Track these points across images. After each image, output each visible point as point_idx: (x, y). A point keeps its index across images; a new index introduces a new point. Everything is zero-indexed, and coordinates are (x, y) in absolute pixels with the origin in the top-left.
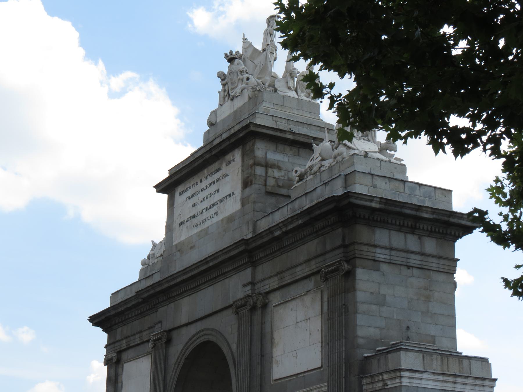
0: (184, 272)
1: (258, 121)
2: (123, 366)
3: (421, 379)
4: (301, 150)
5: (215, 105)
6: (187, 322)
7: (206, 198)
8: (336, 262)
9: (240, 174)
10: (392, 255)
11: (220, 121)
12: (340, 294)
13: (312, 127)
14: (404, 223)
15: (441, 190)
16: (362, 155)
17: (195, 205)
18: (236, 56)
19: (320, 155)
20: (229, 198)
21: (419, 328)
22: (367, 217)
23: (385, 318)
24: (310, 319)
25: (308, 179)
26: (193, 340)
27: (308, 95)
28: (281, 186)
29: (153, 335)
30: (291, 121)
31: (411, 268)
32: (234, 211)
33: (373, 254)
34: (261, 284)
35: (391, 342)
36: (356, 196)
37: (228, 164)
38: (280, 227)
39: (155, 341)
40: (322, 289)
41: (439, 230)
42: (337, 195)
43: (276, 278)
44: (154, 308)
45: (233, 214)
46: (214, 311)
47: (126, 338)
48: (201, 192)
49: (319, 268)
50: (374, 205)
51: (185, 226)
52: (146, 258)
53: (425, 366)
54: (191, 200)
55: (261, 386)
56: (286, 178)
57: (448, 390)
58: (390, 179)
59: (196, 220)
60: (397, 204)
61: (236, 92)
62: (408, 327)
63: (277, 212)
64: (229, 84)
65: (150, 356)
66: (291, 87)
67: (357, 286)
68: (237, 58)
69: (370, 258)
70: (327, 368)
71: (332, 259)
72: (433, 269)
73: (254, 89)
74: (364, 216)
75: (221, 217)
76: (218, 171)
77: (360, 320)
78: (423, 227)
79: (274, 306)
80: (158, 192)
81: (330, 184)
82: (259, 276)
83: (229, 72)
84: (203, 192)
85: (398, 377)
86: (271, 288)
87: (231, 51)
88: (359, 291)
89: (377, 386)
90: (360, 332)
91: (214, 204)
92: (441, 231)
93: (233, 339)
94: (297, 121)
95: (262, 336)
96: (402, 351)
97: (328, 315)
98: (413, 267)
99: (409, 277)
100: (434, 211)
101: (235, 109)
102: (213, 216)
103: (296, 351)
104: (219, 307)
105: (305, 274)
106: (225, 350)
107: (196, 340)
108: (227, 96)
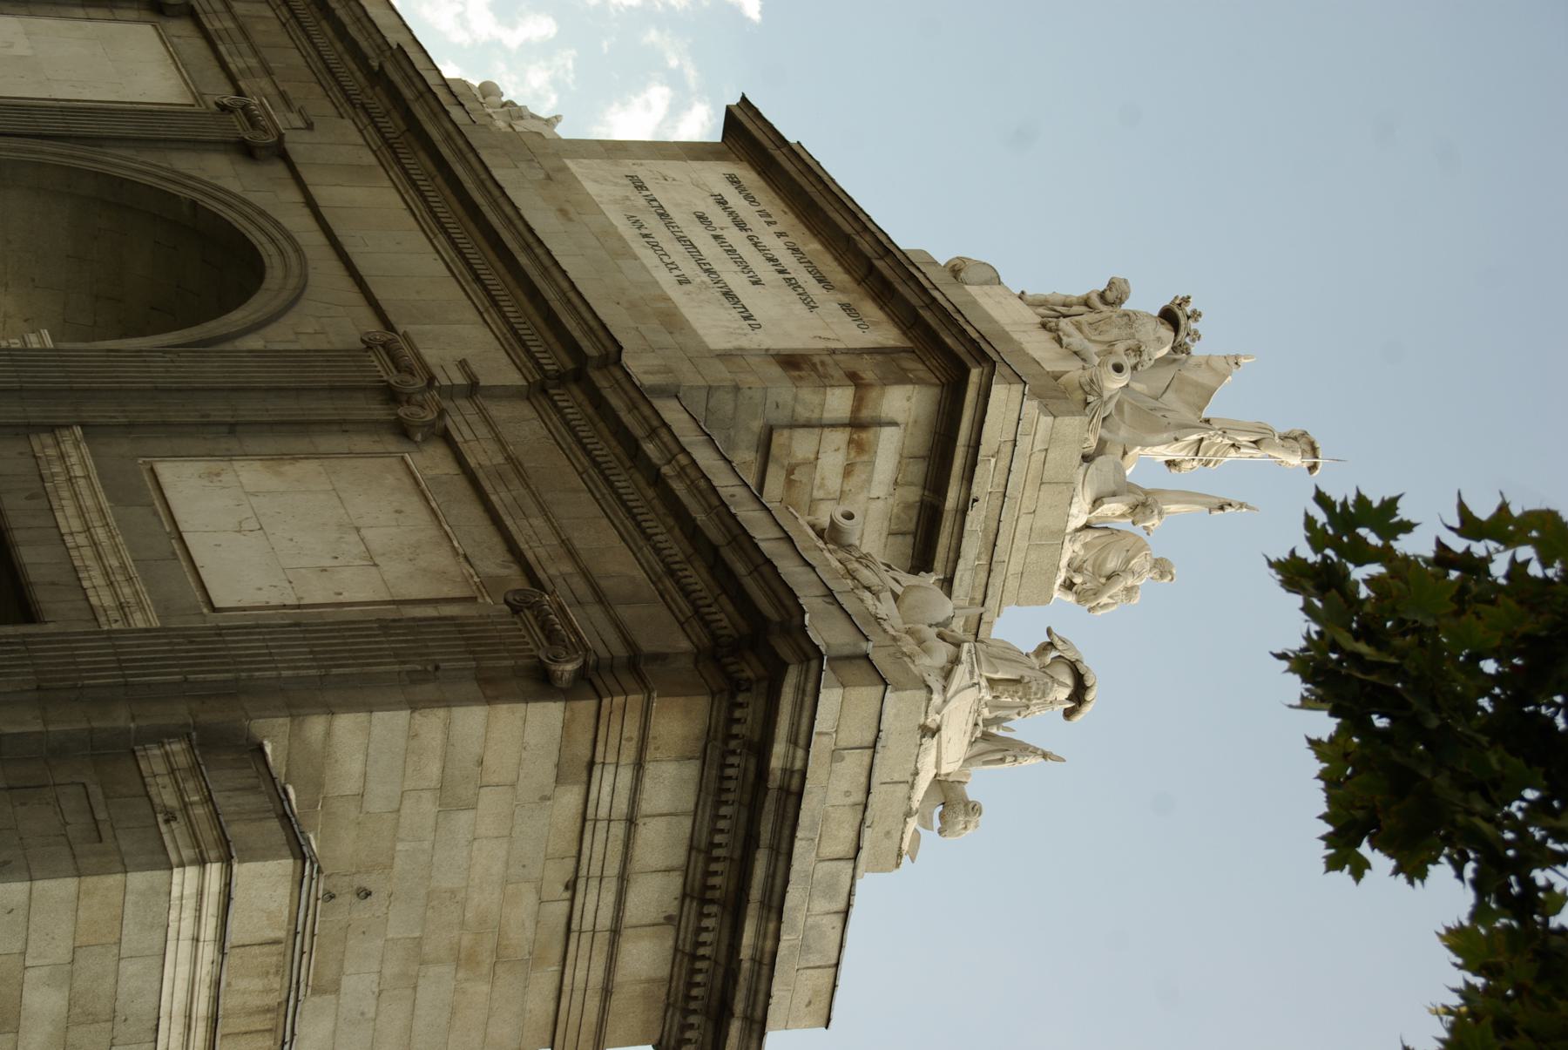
0: (489, 184)
1: (1001, 395)
2: (145, 22)
3: (196, 940)
4: (910, 539)
5: (1014, 281)
6: (320, 202)
7: (731, 251)
8: (577, 633)
9: (821, 345)
10: (612, 824)
11: (970, 295)
12: (471, 652)
13: (983, 575)
14: (717, 859)
15: (830, 986)
16: (926, 718)
17: (702, 218)
18: (1182, 333)
19: (908, 589)
20: (738, 316)
21: (364, 933)
22: (736, 729)
23: (399, 810)
24: (374, 568)
25: (827, 555)
26: (261, 220)
27: (1076, 564)
28: (792, 477)
29: (262, 104)
30: (1000, 503)
31: (567, 895)
32: (701, 332)
33: (611, 758)
34: (473, 417)
35: (316, 838)
36: (810, 686)
38: (674, 457)
39: (245, 109)
40: (480, 600)
41: (698, 985)
42: (807, 622)
43: (500, 459)
44: (350, 103)
45: (690, 327)
46: (368, 280)
47: (242, 30)
48: (745, 234)
49: (549, 587)
50: (779, 749)
51: (630, 191)
52: (504, 99)
53: (243, 949)
54: (718, 209)
55: (130, 426)
56: (817, 494)
57: (156, 1041)
58: (861, 808)
59: (653, 224)
60: (786, 832)
61: (1069, 336)
62: (368, 894)
63: (715, 456)
64: (1092, 317)
65: (190, 100)
66: (1100, 506)
67: (505, 706)
68: (1176, 335)
69: (600, 748)
70: (213, 624)
71: (589, 623)
72: (568, 971)
73: (1091, 388)
74: (738, 721)
76: (820, 281)
77: (390, 723)
78: (706, 929)
79: (403, 458)
80: (729, 110)
81: (834, 609)
82: (500, 411)
83: (1131, 314)
84: (749, 242)
85: (201, 853)
86: (464, 448)
87: (1200, 315)
88: (488, 717)
89: (164, 787)
90: (346, 723)
91: (715, 273)
92: (695, 992)
93: (278, 337)
94: (1001, 524)
95: (302, 426)
96: (295, 864)
97: (394, 621)
98: (572, 900)
99: (539, 891)
100: (766, 964)
101: (1016, 336)
102: (676, 272)
103: (261, 528)
104: (379, 294)
105: (524, 546)
106: (238, 317)
107: (261, 229)
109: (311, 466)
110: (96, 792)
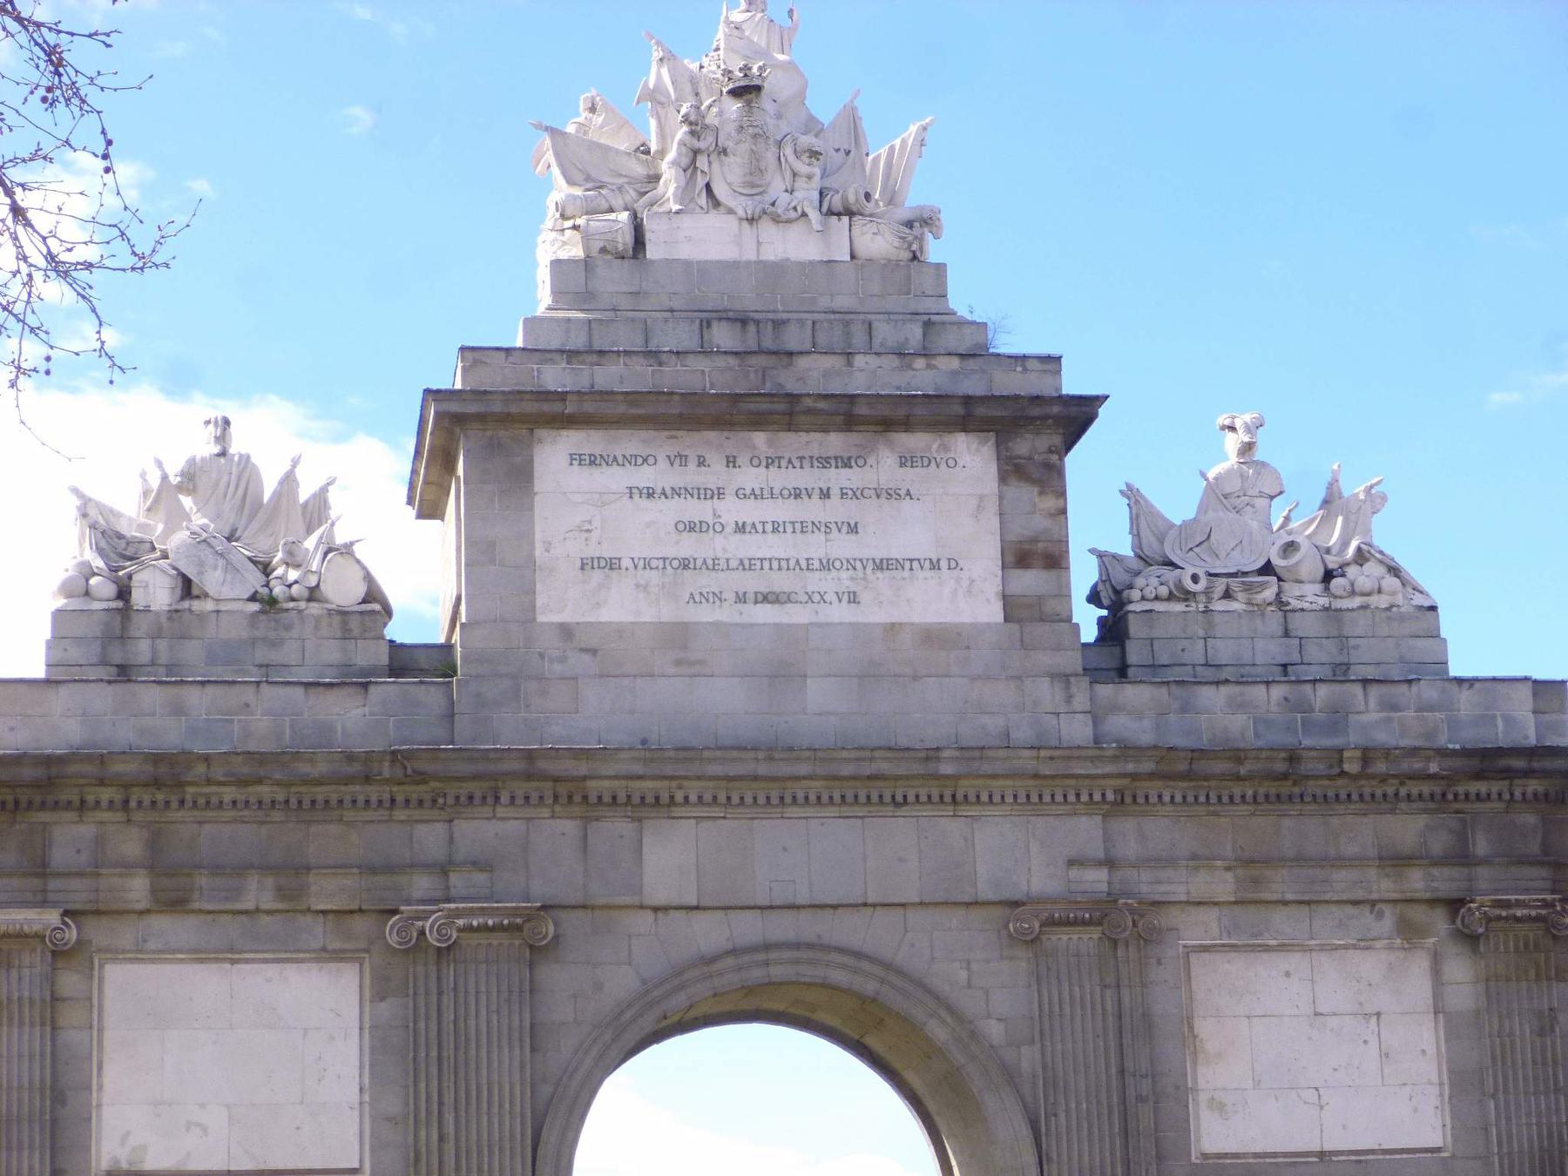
24: (1382, 1016)
48: (730, 499)
75: (873, 613)
76: (847, 465)
108: (704, 191)
109: (1204, 1027)
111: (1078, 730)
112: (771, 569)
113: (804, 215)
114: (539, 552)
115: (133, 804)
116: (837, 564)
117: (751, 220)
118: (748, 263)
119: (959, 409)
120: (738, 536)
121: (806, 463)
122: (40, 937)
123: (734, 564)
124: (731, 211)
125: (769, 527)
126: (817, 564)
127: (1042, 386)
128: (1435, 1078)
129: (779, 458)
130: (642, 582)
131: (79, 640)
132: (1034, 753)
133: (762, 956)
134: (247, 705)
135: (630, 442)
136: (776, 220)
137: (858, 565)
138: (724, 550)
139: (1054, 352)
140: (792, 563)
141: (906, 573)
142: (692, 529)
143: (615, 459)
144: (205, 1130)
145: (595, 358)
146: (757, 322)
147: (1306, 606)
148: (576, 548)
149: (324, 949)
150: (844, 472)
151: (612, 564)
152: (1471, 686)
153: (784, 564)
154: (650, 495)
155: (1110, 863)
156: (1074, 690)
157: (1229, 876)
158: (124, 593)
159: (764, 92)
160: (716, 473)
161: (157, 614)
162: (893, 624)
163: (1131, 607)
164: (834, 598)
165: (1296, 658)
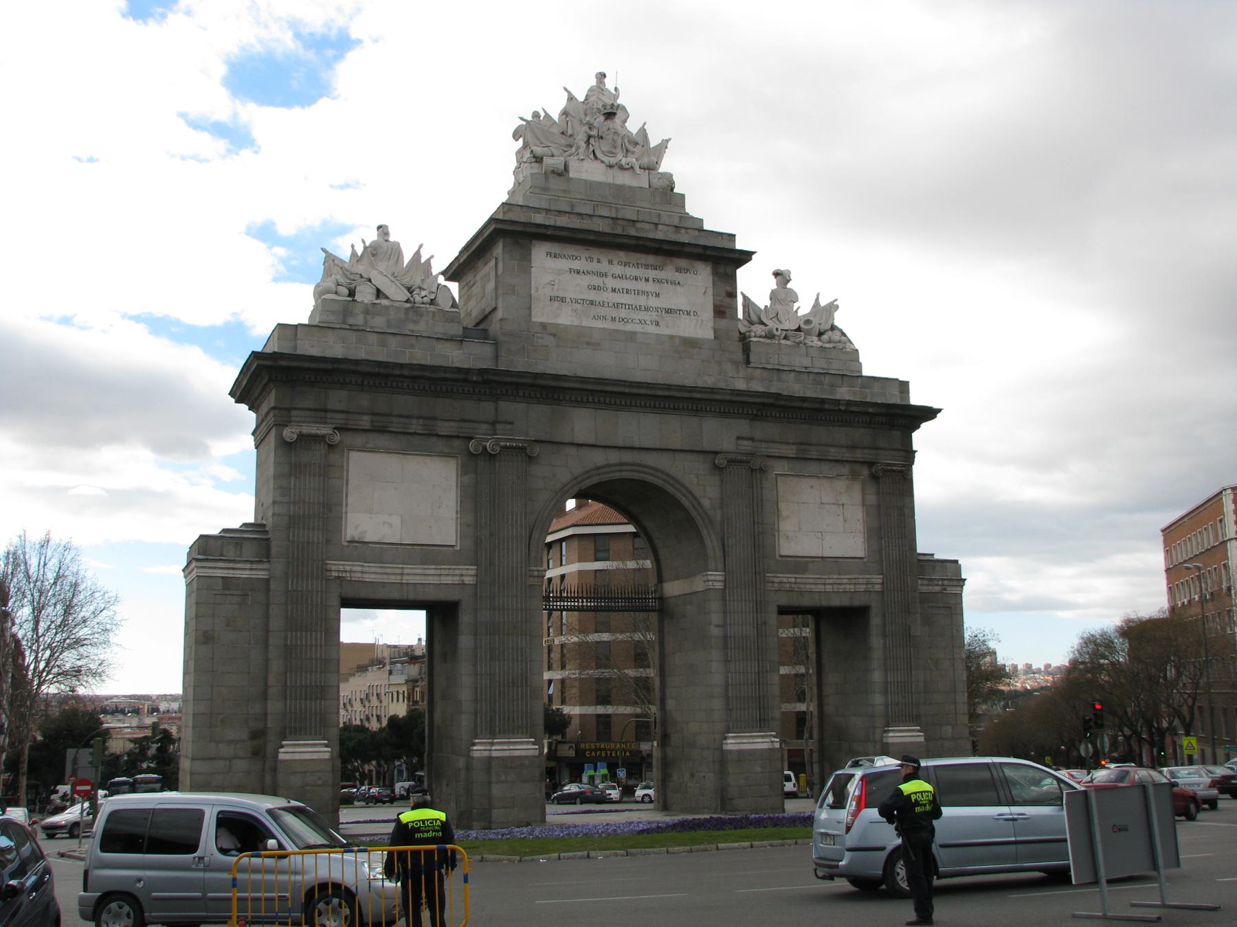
24: (845, 507)
37: (679, 270)
109: (782, 506)
110: (931, 605)
111: (741, 385)
112: (625, 308)
113: (632, 167)
114: (533, 292)
115: (366, 383)
116: (651, 309)
117: (611, 166)
118: (610, 184)
119: (701, 251)
120: (613, 293)
121: (640, 267)
122: (323, 437)
123: (611, 305)
124: (603, 162)
125: (625, 291)
126: (643, 309)
127: (727, 245)
128: (862, 530)
129: (630, 263)
130: (575, 308)
131: (333, 312)
132: (732, 392)
133: (619, 468)
134: (412, 345)
135: (571, 250)
136: (621, 168)
137: (659, 310)
138: (607, 298)
139: (733, 233)
140: (634, 307)
141: (678, 315)
142: (594, 289)
143: (564, 256)
144: (391, 525)
145: (557, 213)
146: (616, 207)
147: (814, 345)
148: (547, 292)
149: (442, 452)
150: (654, 272)
151: (563, 300)
152: (878, 381)
153: (630, 307)
154: (578, 272)
155: (752, 439)
156: (740, 368)
157: (794, 447)
158: (352, 293)
159: (617, 117)
160: (604, 266)
161: (367, 304)
162: (672, 336)
163: (752, 339)
164: (650, 324)
165: (810, 365)
